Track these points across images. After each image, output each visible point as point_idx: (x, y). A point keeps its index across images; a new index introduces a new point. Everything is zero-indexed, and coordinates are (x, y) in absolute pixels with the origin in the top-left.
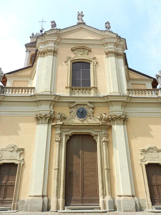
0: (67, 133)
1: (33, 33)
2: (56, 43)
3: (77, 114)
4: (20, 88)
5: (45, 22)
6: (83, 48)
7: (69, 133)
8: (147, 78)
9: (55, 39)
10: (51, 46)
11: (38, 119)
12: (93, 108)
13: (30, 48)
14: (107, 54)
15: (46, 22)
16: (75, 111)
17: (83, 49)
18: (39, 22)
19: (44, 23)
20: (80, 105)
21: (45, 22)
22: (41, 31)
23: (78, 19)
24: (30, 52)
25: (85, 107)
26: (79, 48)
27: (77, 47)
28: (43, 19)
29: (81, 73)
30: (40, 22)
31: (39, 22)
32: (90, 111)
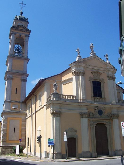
0: (95, 123)
1: (16, 16)
2: (84, 67)
3: (98, 113)
4: (68, 95)
5: (24, 4)
6: (96, 72)
7: (97, 123)
8: (121, 89)
9: (84, 65)
10: (81, 69)
11: (82, 115)
12: (105, 110)
13: (15, 31)
14: (109, 77)
15: (25, 5)
16: (97, 111)
17: (98, 73)
18: (19, 3)
19: (24, 5)
20: (99, 108)
21: (24, 4)
22: (22, 13)
23: (91, 49)
24: (15, 34)
25: (101, 109)
26: (95, 72)
27: (95, 71)
28: (22, 1)
29: (97, 89)
30: (20, 3)
31: (19, 3)
32: (103, 111)
